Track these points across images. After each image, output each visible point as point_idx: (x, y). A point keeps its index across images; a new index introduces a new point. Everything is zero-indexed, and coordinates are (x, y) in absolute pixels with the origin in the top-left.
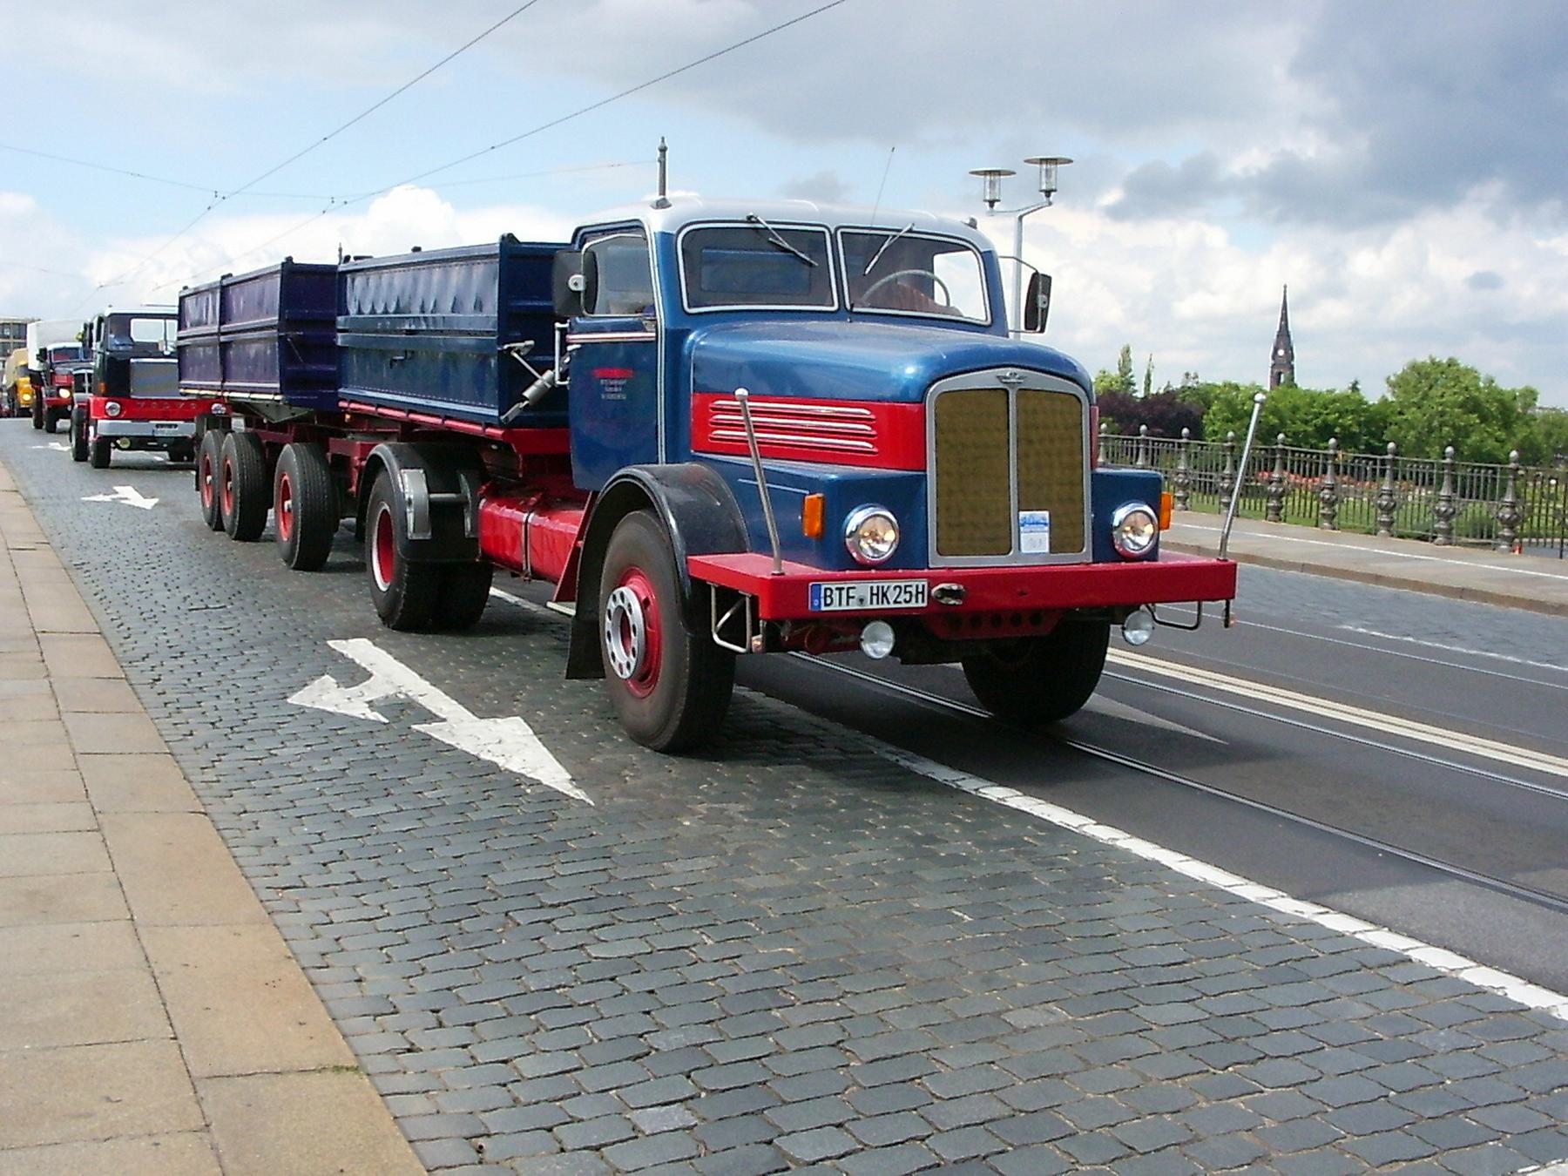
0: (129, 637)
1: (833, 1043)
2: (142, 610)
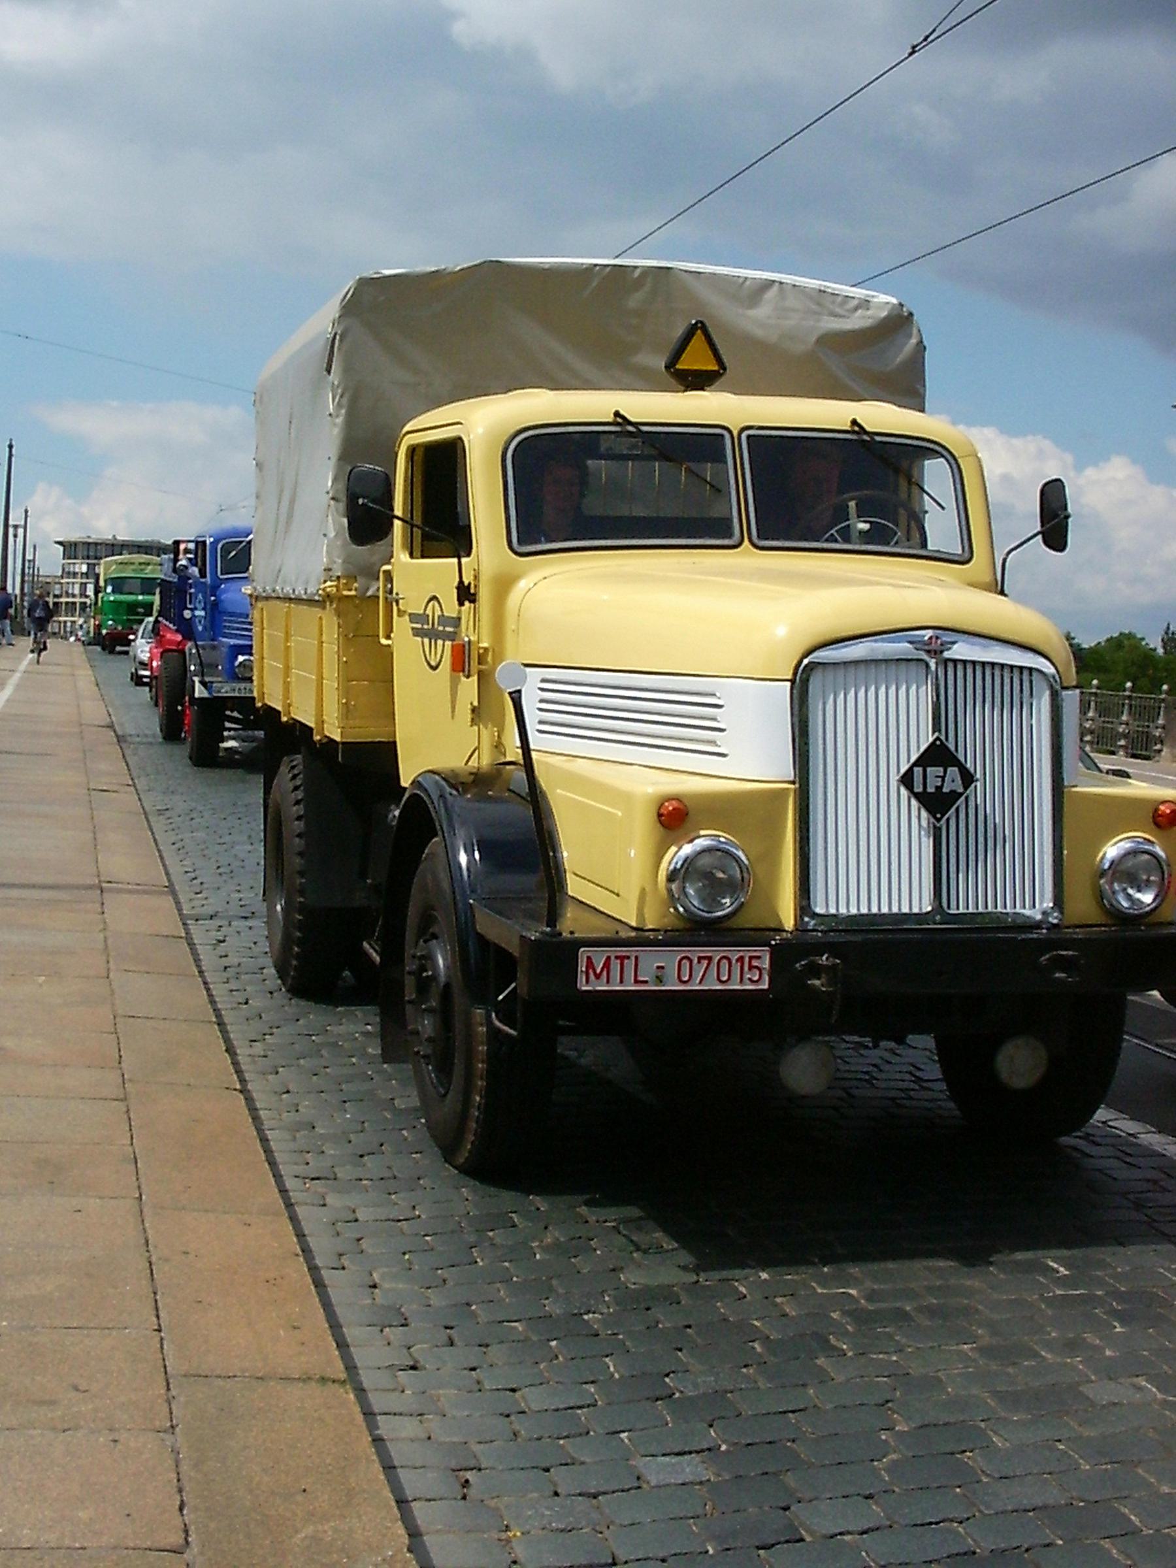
0: (200, 893)
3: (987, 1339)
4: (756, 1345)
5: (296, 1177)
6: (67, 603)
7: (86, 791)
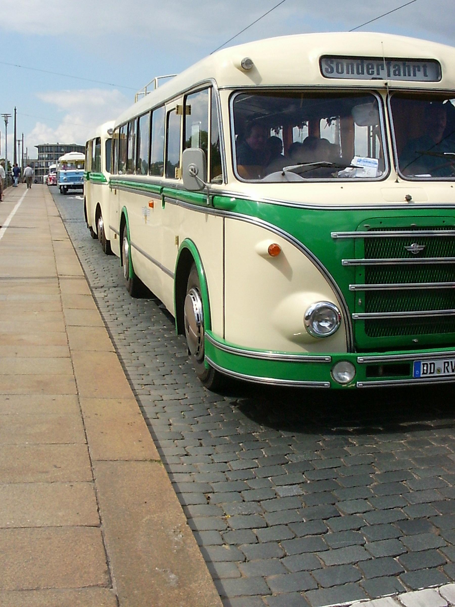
0: (97, 278)
3: (411, 438)
4: (320, 443)
5: (139, 384)
6: (40, 170)
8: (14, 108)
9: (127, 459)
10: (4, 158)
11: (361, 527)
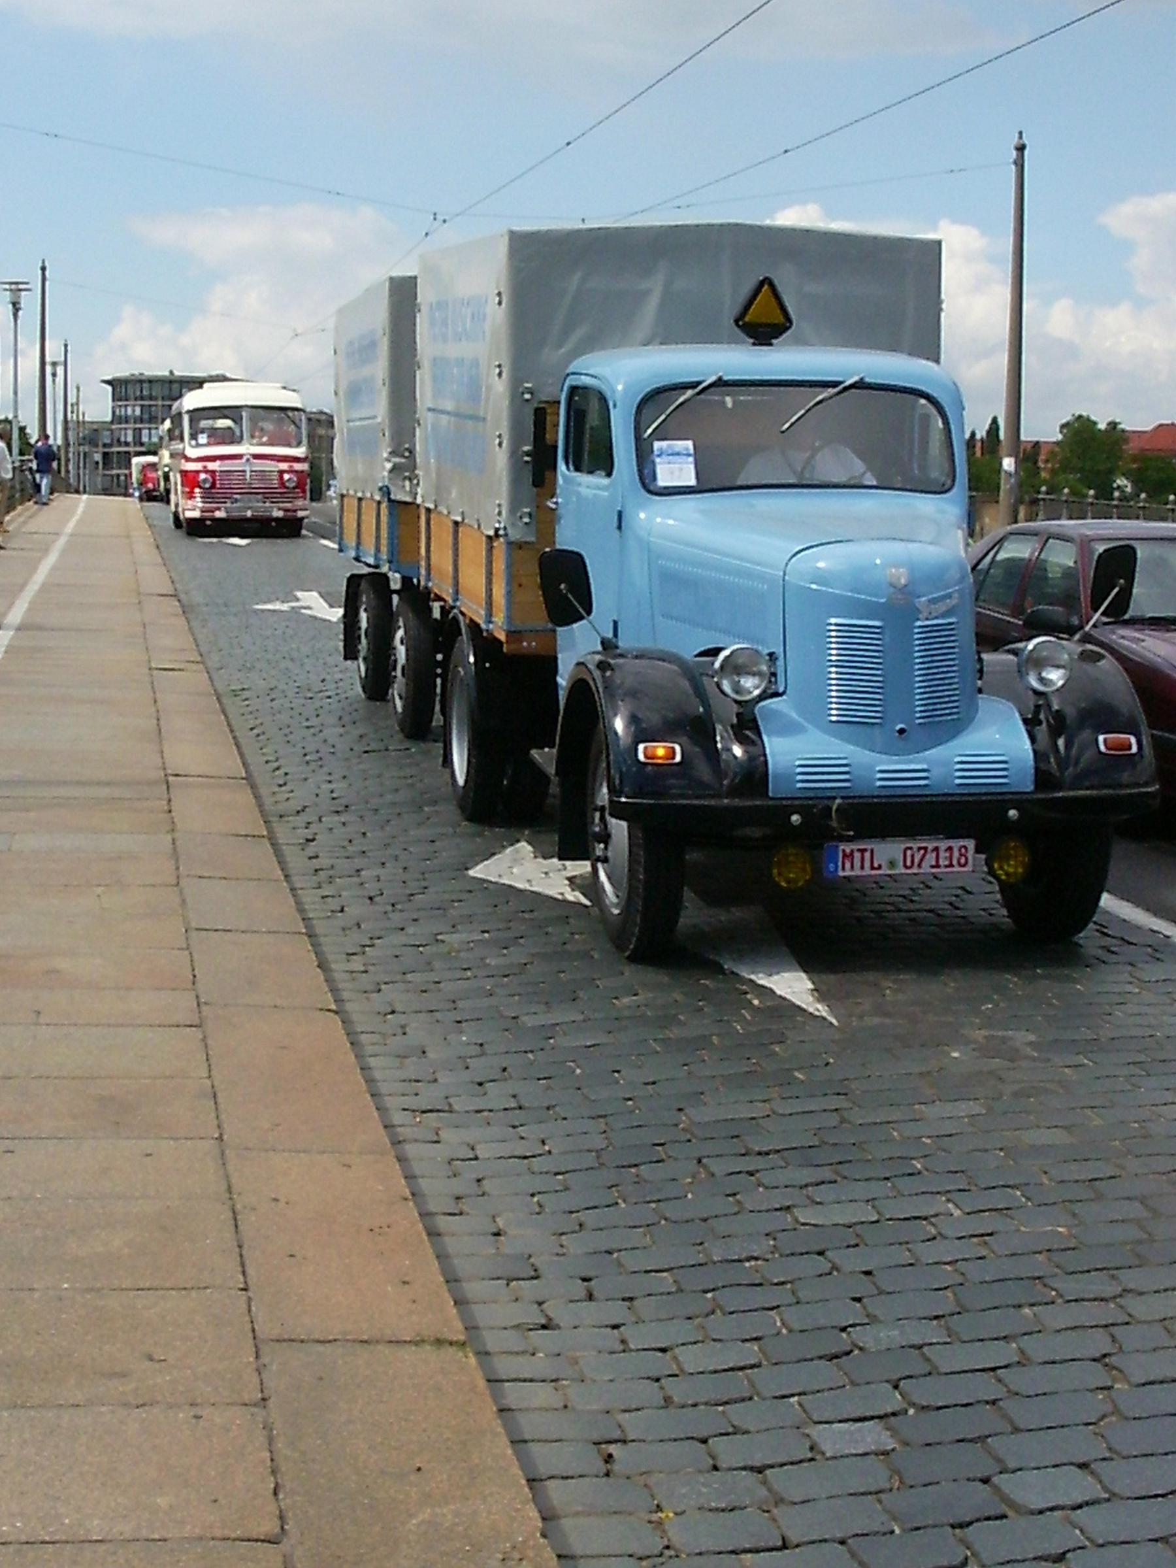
0: (285, 784)
1: (1097, 1355)
2: (307, 750)
5: (404, 1110)
6: (119, 453)
7: (147, 671)
8: (40, 264)
9: (365, 1337)
10: (10, 417)
11: (1069, 1551)
